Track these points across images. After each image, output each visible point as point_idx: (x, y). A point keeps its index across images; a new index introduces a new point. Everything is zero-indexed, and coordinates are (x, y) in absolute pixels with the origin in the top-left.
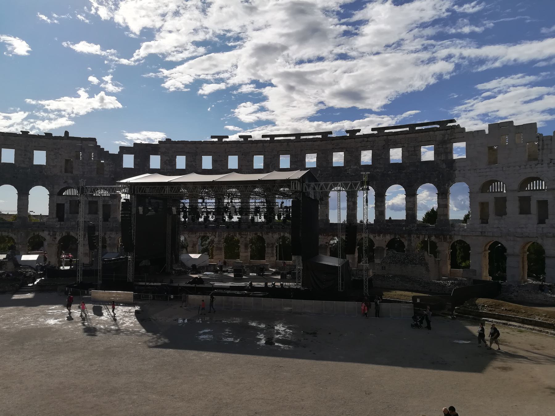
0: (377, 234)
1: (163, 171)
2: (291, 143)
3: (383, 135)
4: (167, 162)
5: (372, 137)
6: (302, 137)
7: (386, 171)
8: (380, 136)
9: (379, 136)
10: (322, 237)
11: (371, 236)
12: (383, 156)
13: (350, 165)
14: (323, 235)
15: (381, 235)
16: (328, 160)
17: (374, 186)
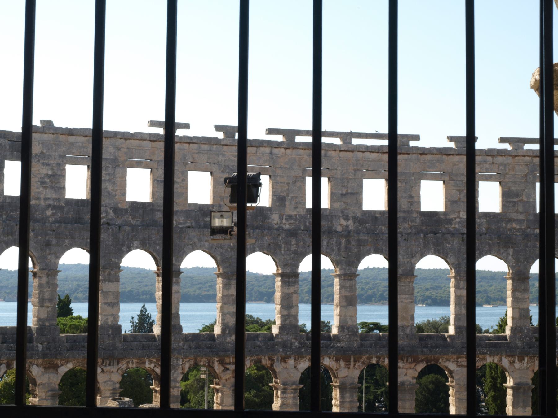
0: (517, 358)
1: (37, 202)
2: (334, 152)
3: (526, 155)
4: (47, 180)
5: (502, 156)
6: (355, 142)
7: (530, 228)
8: (519, 156)
9: (516, 156)
10: (404, 364)
11: (505, 362)
12: (524, 196)
13: (458, 211)
14: (407, 361)
15: (526, 359)
16: (412, 197)
17: (510, 257)
